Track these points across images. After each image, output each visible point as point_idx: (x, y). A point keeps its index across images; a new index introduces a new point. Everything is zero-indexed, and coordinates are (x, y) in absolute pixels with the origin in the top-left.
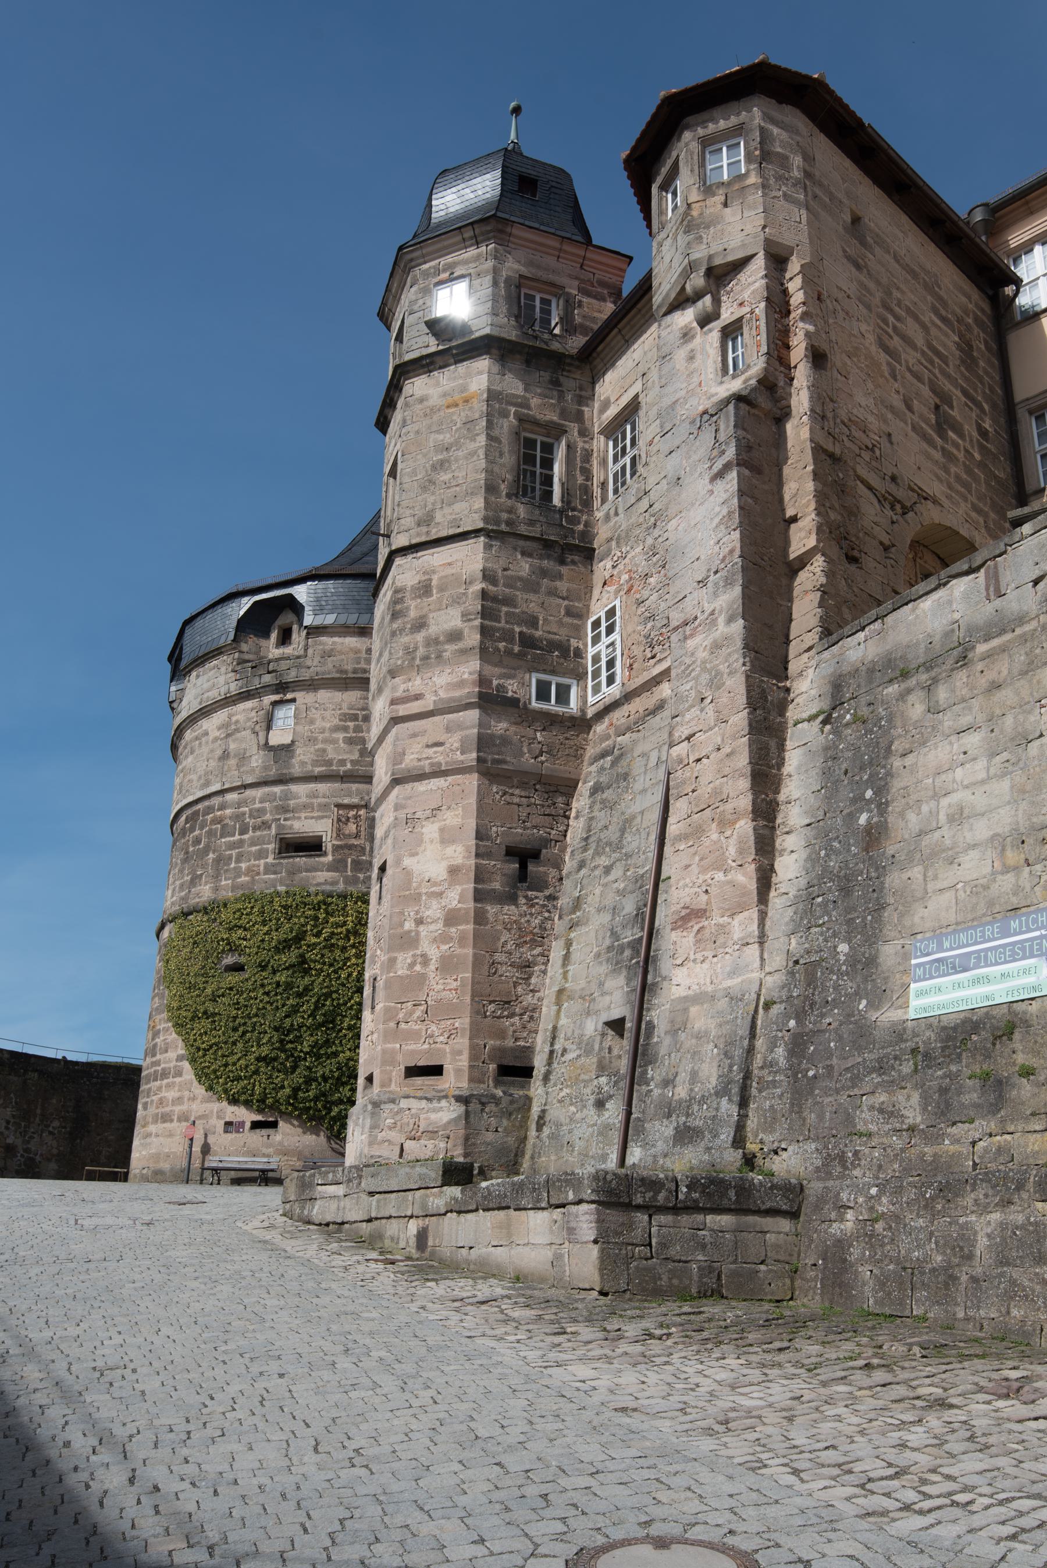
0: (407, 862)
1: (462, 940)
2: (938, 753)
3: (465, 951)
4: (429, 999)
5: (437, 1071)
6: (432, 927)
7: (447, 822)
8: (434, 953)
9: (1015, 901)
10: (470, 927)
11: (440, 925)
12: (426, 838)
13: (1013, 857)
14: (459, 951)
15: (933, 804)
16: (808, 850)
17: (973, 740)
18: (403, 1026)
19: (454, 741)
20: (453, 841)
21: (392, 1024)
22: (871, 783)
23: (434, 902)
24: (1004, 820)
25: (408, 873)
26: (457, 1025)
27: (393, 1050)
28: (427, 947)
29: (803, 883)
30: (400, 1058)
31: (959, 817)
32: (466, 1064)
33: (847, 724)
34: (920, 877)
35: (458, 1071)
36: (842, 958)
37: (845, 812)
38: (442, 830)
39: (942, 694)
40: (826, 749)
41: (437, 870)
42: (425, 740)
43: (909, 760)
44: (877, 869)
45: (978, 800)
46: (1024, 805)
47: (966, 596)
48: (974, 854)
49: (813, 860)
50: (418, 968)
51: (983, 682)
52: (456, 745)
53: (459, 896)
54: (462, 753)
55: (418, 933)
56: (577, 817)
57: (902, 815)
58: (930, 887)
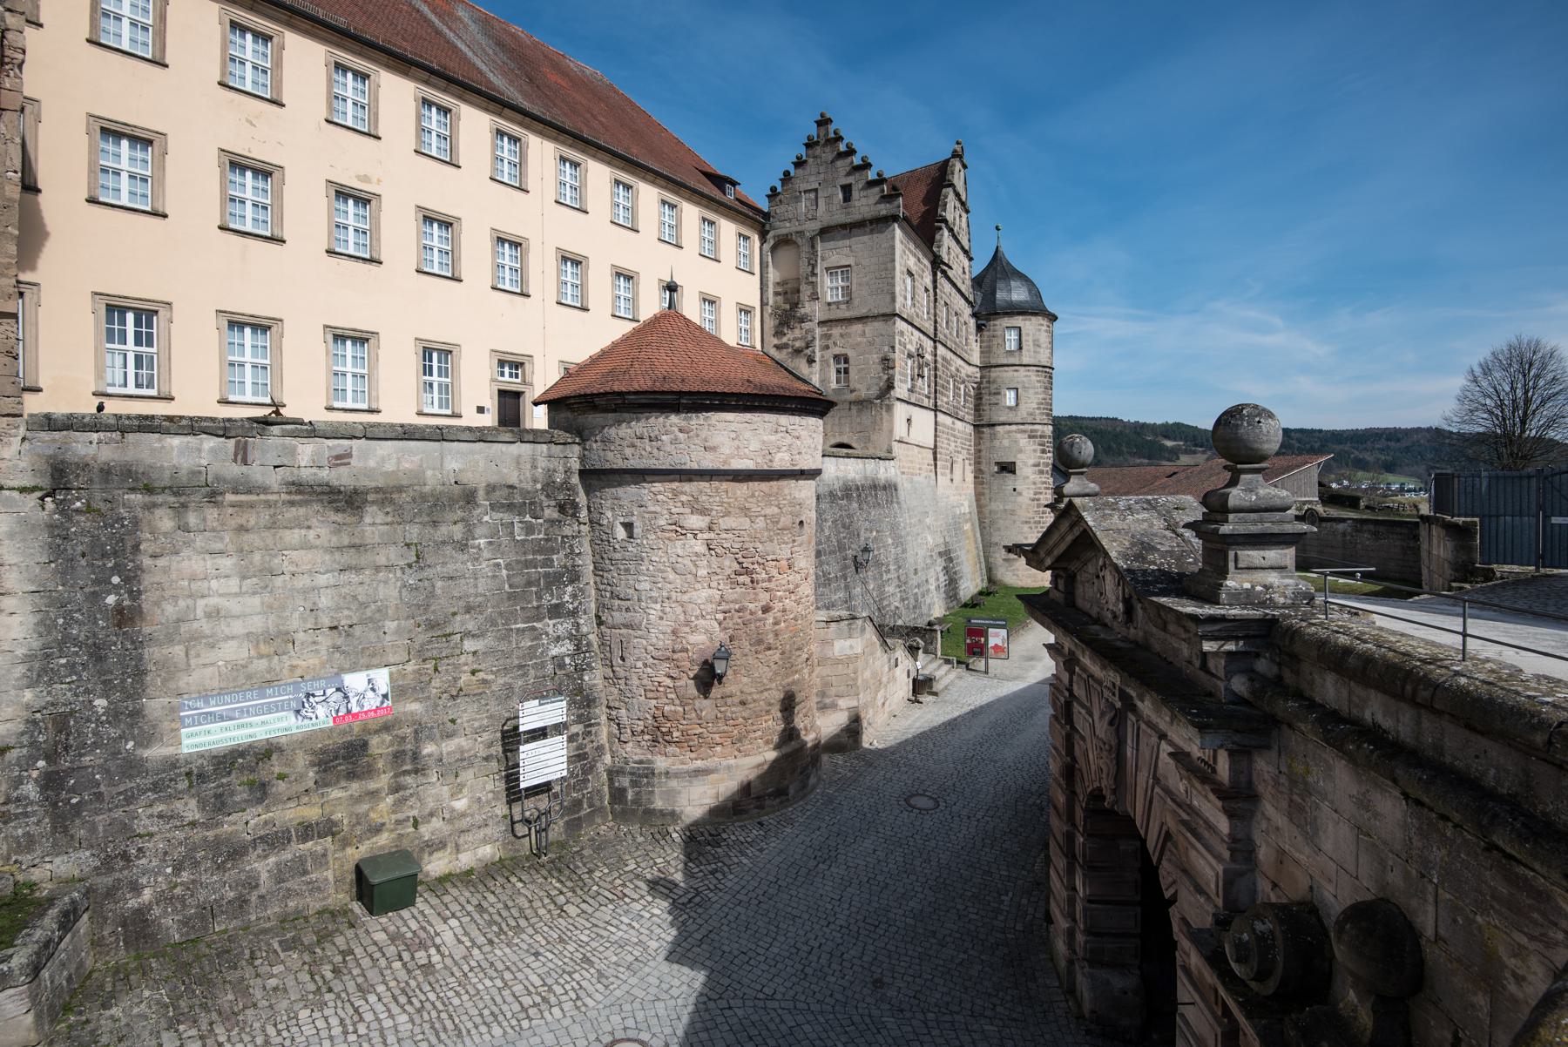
2: (191, 563)
9: (268, 677)
13: (264, 649)
15: (190, 602)
16: (39, 616)
17: (226, 563)
22: (117, 569)
24: (257, 623)
29: (36, 644)
31: (215, 614)
33: (77, 511)
34: (182, 654)
36: (101, 711)
37: (87, 590)
39: (192, 519)
40: (51, 526)
43: (161, 562)
44: (133, 642)
45: (232, 605)
46: (272, 617)
47: (212, 450)
48: (231, 643)
49: (44, 626)
51: (233, 523)
57: (157, 604)
58: (192, 662)
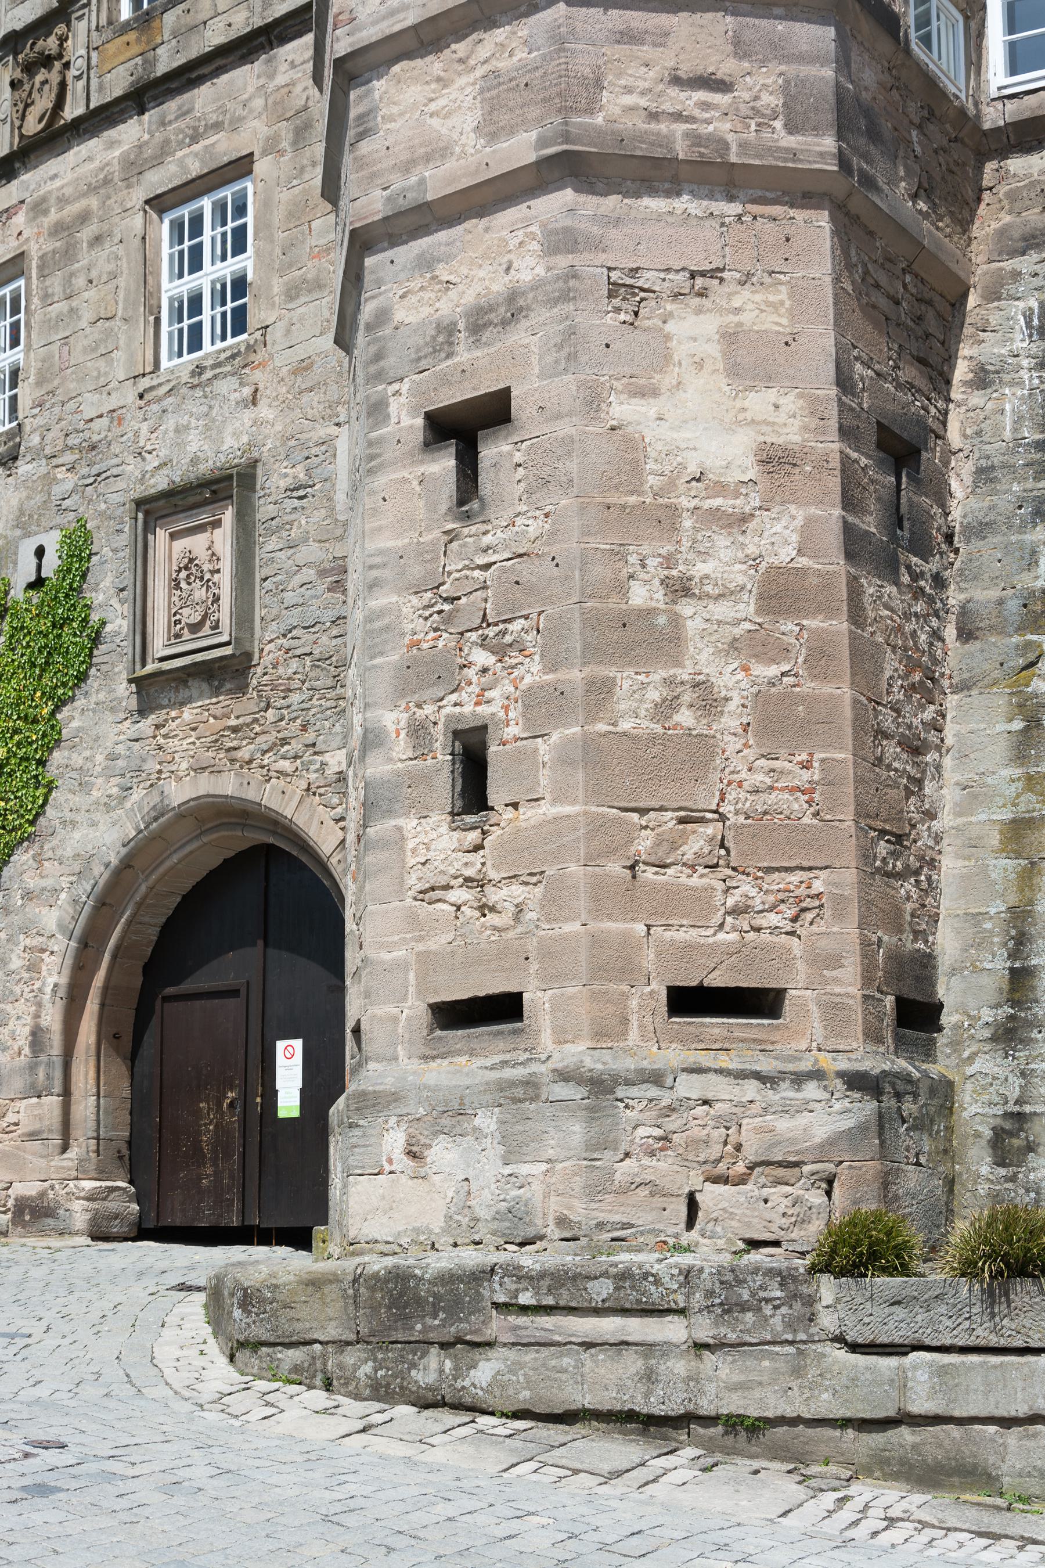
0: (622, 409)
1: (818, 656)
3: (829, 689)
4: (726, 809)
5: (758, 1003)
6: (722, 610)
7: (746, 318)
8: (730, 680)
10: (840, 625)
11: (747, 607)
12: (681, 351)
14: (809, 687)
18: (648, 874)
19: (762, 85)
20: (769, 380)
21: (616, 868)
23: (722, 541)
25: (628, 445)
26: (818, 886)
27: (625, 941)
28: (702, 658)
30: (649, 959)
32: (855, 990)
35: (833, 1010)
38: (730, 337)
41: (731, 454)
42: (666, 59)
50: (685, 717)
52: (770, 100)
53: (798, 531)
54: (791, 128)
55: (676, 621)
56: (982, 379)
